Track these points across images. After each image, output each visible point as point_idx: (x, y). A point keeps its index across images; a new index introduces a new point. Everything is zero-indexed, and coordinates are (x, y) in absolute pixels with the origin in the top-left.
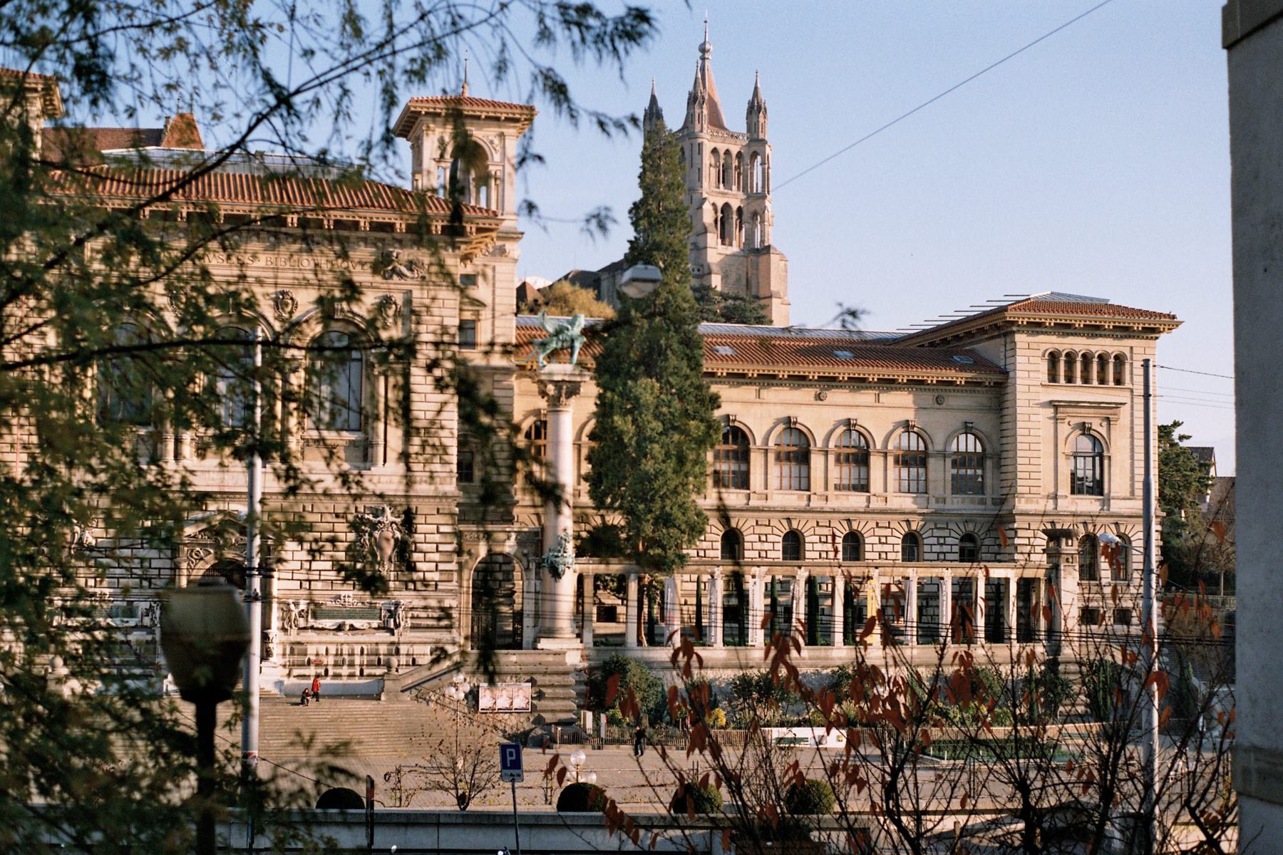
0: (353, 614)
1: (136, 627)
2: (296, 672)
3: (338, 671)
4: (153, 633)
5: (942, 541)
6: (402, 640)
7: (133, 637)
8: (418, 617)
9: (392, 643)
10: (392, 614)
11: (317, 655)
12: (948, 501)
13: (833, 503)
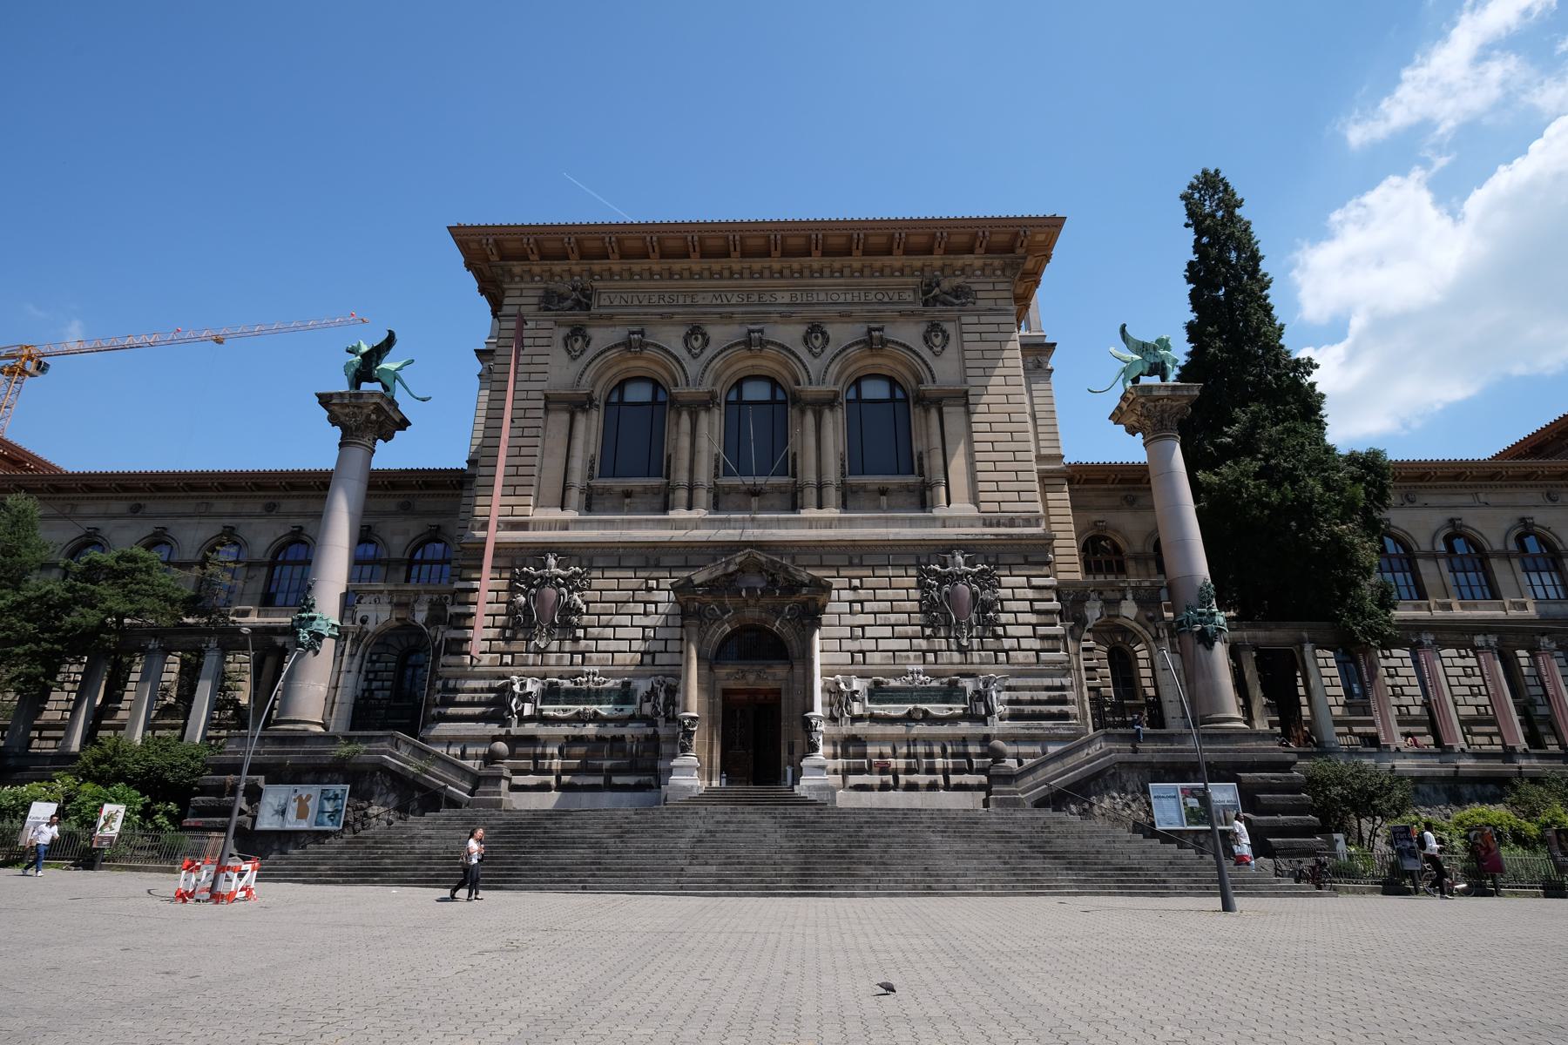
0: (926, 695)
1: (632, 718)
2: (854, 779)
3: (914, 778)
7: (629, 731)
8: (1018, 702)
10: (981, 696)
11: (881, 756)
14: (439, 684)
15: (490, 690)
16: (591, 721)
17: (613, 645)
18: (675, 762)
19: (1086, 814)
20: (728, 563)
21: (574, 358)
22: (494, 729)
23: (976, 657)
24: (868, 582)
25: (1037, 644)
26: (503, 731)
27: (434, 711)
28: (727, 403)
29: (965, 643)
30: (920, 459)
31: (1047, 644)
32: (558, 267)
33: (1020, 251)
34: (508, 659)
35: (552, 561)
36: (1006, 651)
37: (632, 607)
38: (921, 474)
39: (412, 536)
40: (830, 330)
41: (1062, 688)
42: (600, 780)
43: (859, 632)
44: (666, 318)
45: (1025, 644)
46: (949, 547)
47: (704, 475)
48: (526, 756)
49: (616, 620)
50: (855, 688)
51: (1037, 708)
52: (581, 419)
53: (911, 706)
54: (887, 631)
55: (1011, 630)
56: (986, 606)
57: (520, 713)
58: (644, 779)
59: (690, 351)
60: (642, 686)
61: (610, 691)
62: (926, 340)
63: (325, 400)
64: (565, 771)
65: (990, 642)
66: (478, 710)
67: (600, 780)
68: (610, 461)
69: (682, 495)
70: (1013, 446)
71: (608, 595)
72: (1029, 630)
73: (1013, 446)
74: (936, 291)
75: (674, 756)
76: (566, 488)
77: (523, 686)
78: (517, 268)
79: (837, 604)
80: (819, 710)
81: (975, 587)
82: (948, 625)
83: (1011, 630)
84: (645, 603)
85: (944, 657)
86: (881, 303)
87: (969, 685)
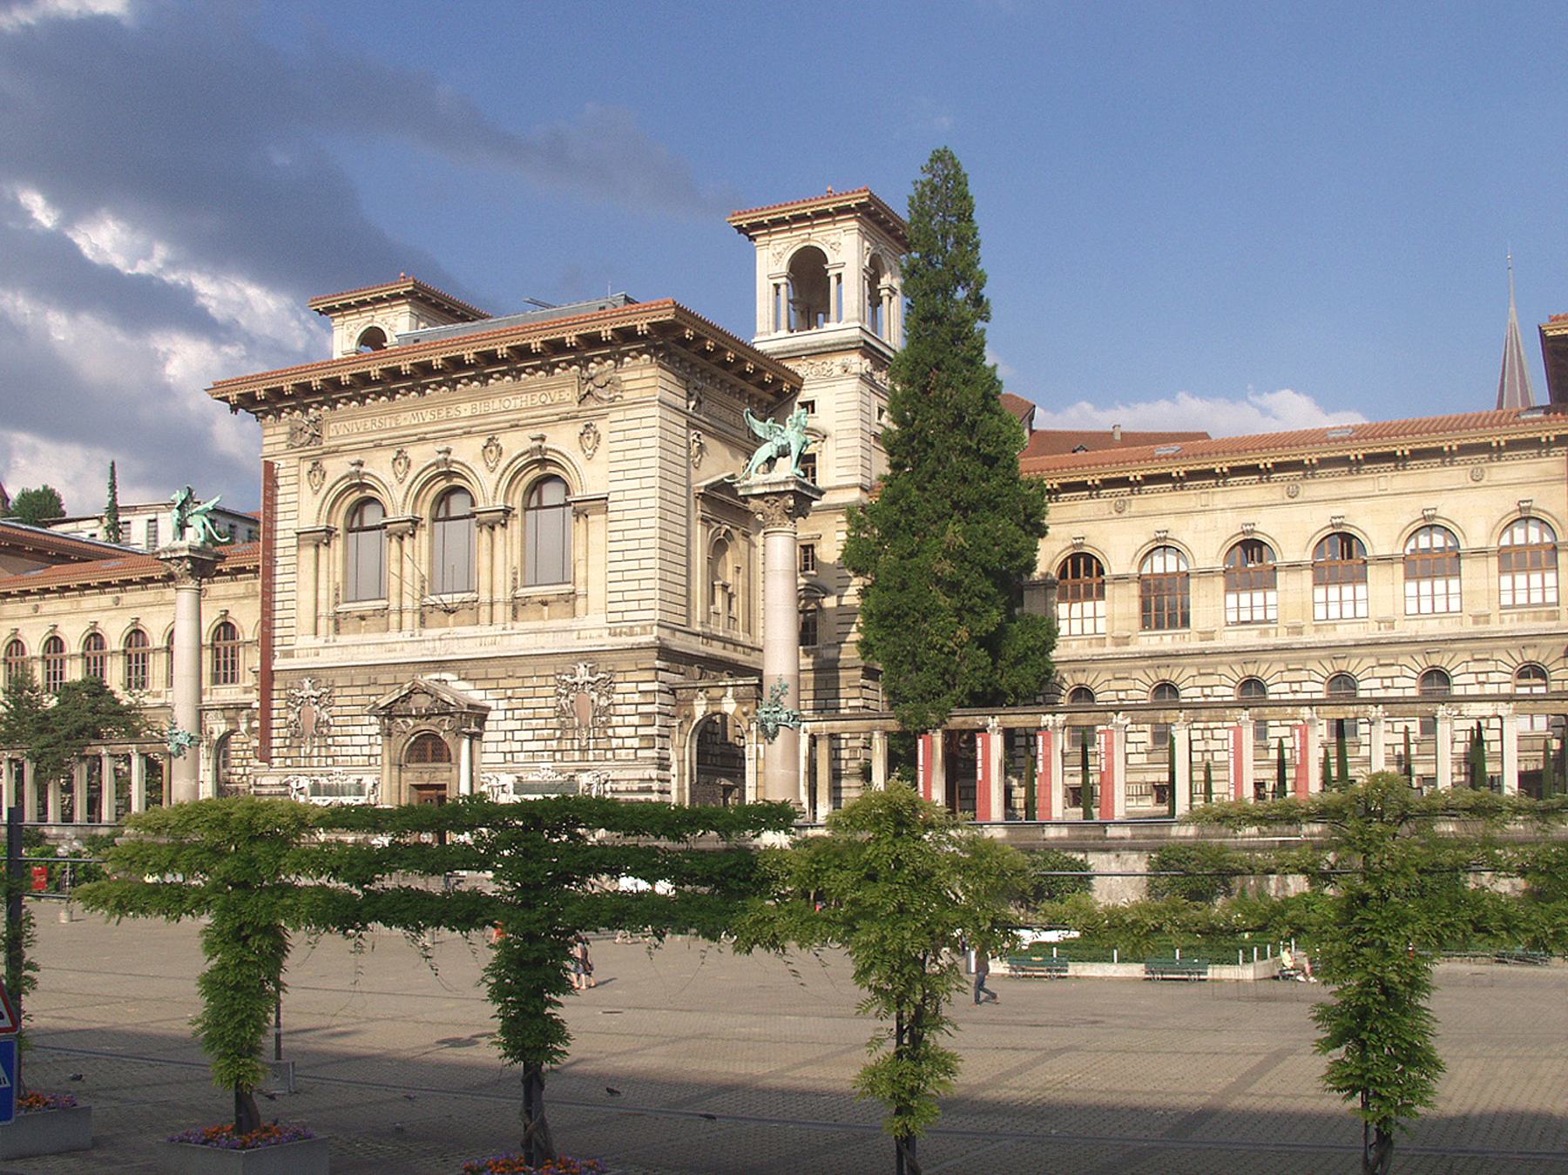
5: (1482, 678)
8: (617, 791)
12: (1494, 618)
13: (1310, 637)
20: (401, 688)
25: (636, 743)
35: (307, 685)
41: (651, 780)
43: (509, 735)
45: (628, 743)
46: (584, 655)
47: (408, 603)
52: (322, 549)
54: (529, 735)
56: (604, 711)
65: (603, 743)
68: (350, 588)
69: (394, 618)
76: (316, 619)
81: (594, 695)
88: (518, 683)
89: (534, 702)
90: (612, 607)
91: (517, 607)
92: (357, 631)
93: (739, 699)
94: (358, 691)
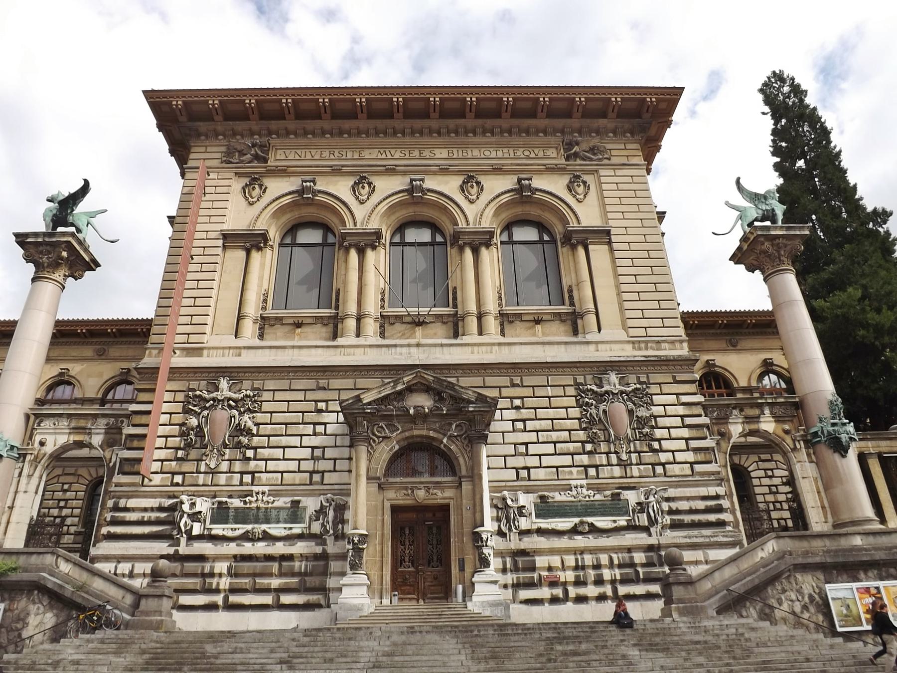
0: (591, 509)
1: (300, 537)
2: (524, 594)
3: (582, 591)
4: (324, 543)
6: (663, 541)
8: (678, 512)
9: (650, 548)
14: (110, 503)
15: (161, 509)
16: (259, 540)
17: (282, 466)
18: (345, 580)
19: (767, 615)
21: (251, 204)
22: (163, 548)
23: (635, 471)
24: (529, 402)
25: (690, 457)
26: (171, 551)
27: (104, 530)
28: (392, 244)
29: (624, 457)
30: (570, 291)
31: (700, 457)
32: (240, 126)
33: (646, 116)
34: (178, 479)
36: (663, 465)
37: (302, 429)
38: (572, 304)
39: (106, 378)
40: (485, 180)
41: (717, 497)
42: (268, 599)
43: (522, 449)
44: (336, 171)
45: (680, 457)
48: (194, 575)
49: (284, 441)
50: (521, 503)
51: (696, 518)
53: (577, 520)
54: (550, 448)
55: (666, 445)
56: (642, 422)
57: (189, 532)
58: (313, 598)
59: (357, 198)
60: (311, 504)
61: (279, 509)
62: (570, 189)
63: (21, 239)
64: (233, 590)
65: (648, 457)
66: (146, 530)
67: (268, 599)
69: (351, 323)
70: (654, 279)
71: (277, 418)
72: (682, 444)
73: (654, 279)
74: (576, 149)
75: (343, 574)
76: (240, 318)
77: (193, 505)
78: (203, 126)
79: (501, 422)
80: (489, 526)
81: (631, 406)
82: (608, 441)
83: (666, 445)
84: (315, 424)
85: (605, 472)
86: (528, 158)
87: (632, 498)
88: (528, 392)
89: (551, 413)
90: (630, 323)
91: (506, 319)
92: (290, 335)
93: (778, 419)
94: (300, 396)
